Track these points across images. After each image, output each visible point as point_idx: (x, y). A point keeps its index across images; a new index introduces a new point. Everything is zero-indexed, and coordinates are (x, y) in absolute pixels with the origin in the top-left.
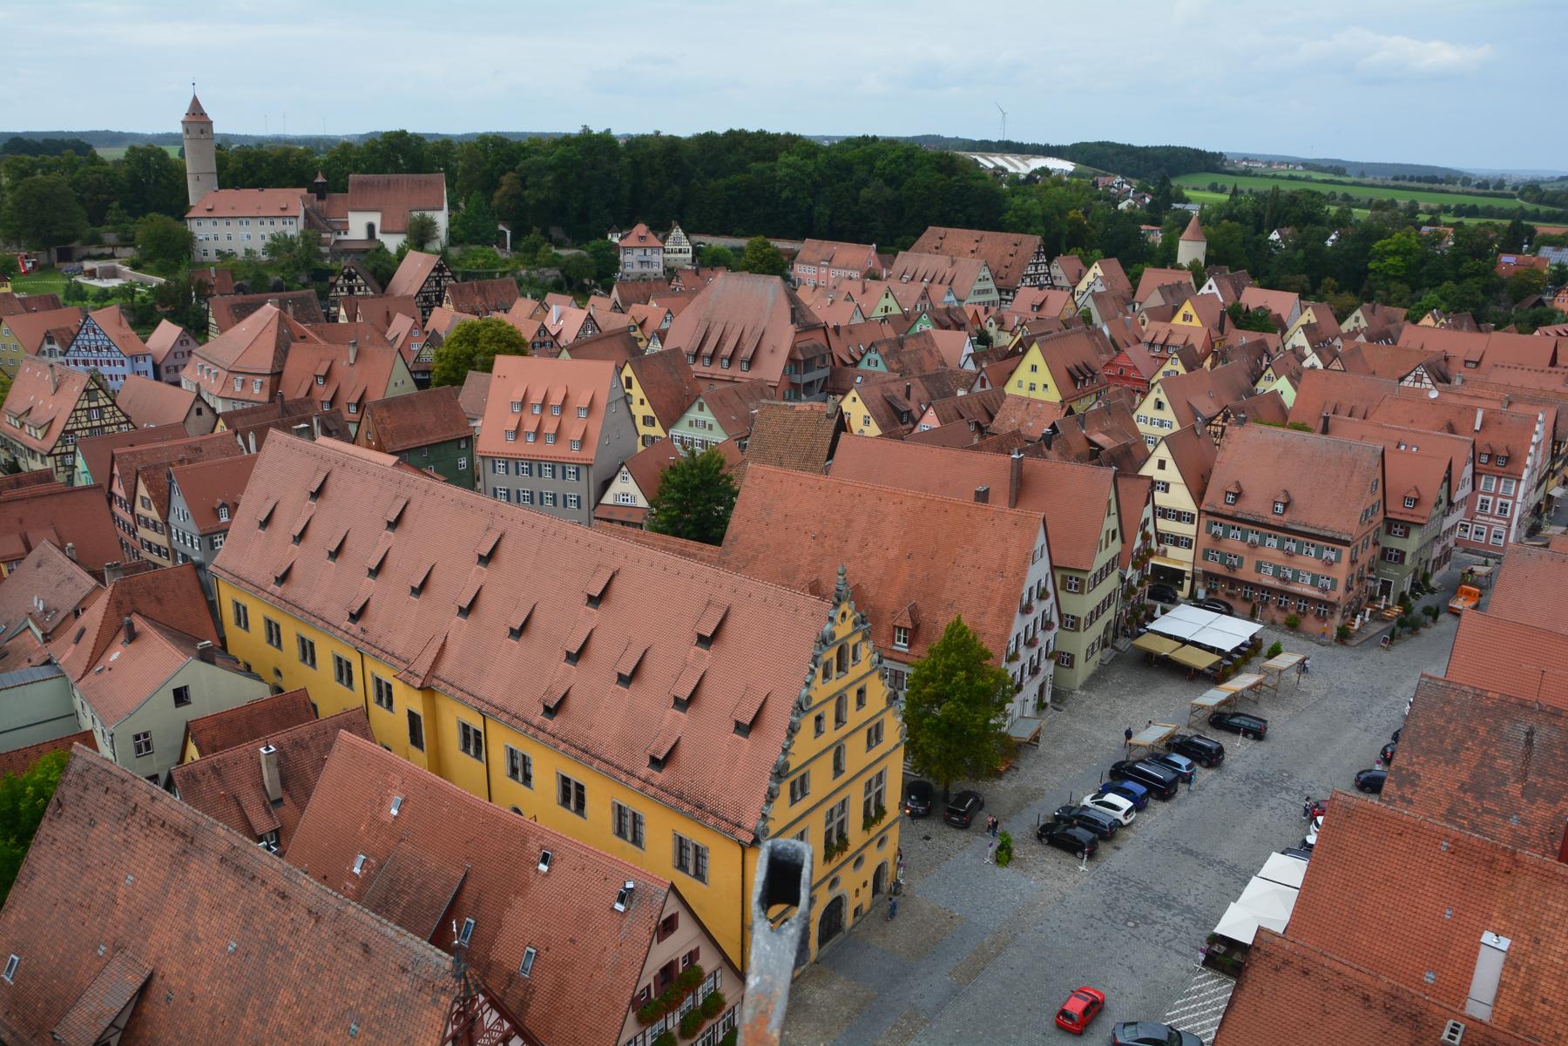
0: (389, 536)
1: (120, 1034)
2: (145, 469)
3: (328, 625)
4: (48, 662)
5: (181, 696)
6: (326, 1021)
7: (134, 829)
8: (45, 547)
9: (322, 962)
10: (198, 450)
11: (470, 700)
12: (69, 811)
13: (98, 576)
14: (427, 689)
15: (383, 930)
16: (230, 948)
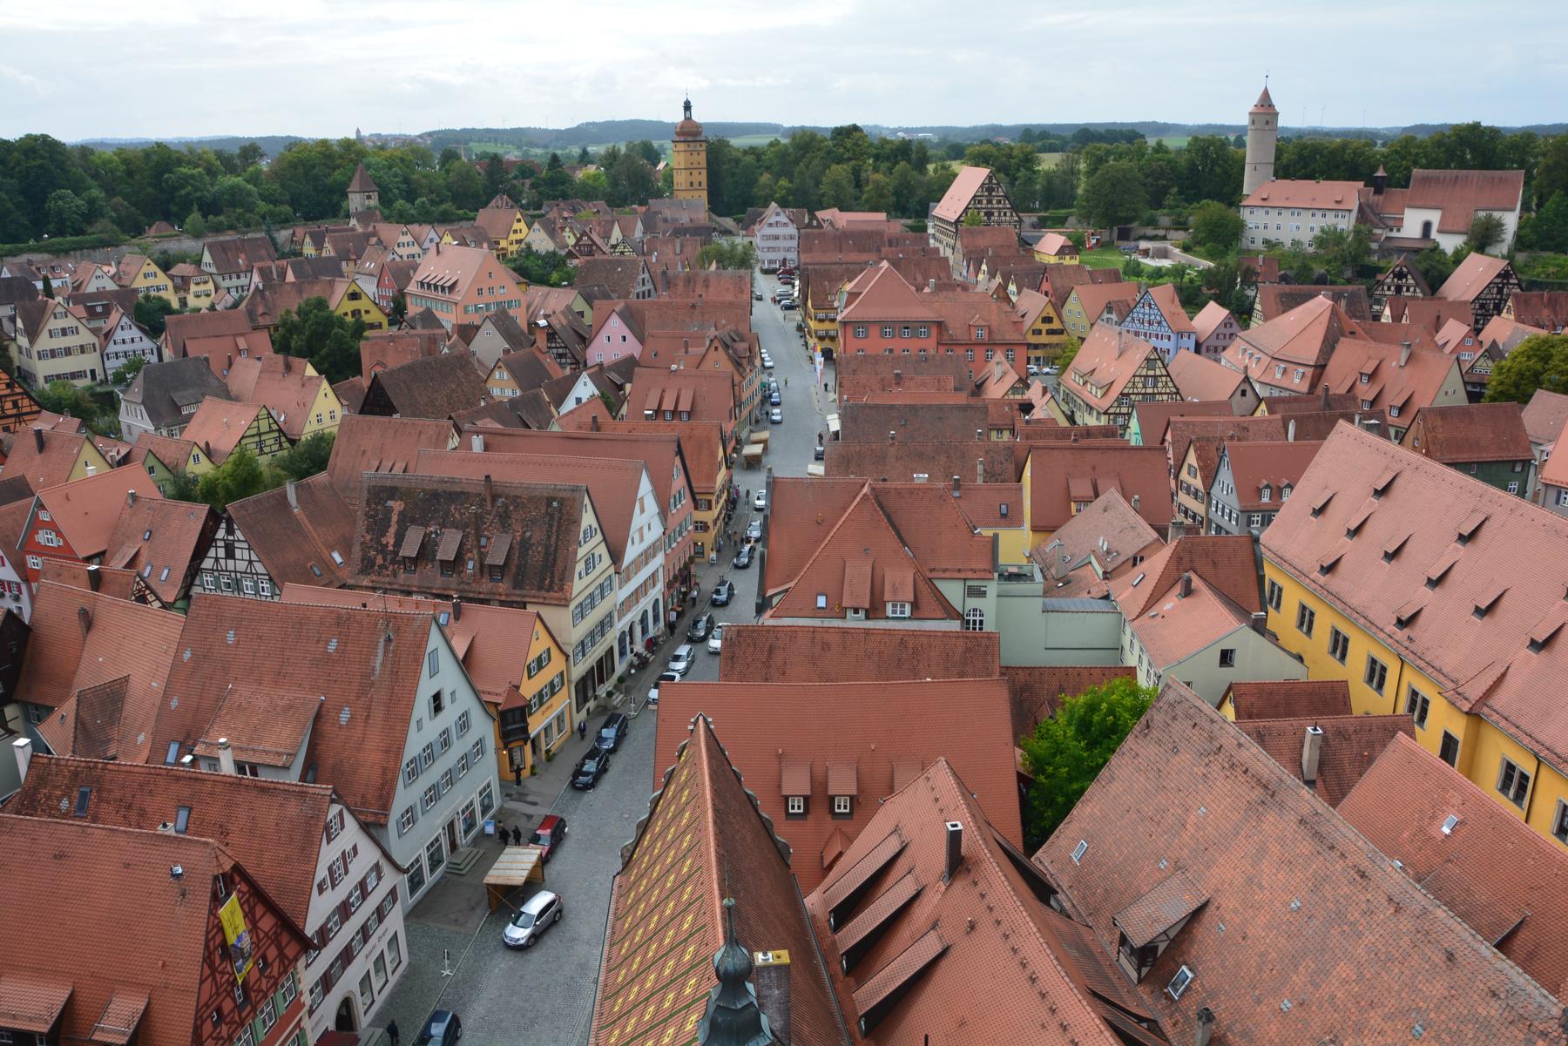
0: (1457, 550)
1: (1167, 943)
2: (1198, 439)
3: (1370, 627)
4: (1106, 597)
5: (1226, 657)
6: (1386, 1010)
7: (1215, 767)
8: (1111, 495)
9: (1394, 952)
10: (1246, 429)
11: (1527, 740)
12: (1155, 734)
13: (1162, 532)
14: (1473, 716)
15: (1476, 946)
16: (1293, 905)
